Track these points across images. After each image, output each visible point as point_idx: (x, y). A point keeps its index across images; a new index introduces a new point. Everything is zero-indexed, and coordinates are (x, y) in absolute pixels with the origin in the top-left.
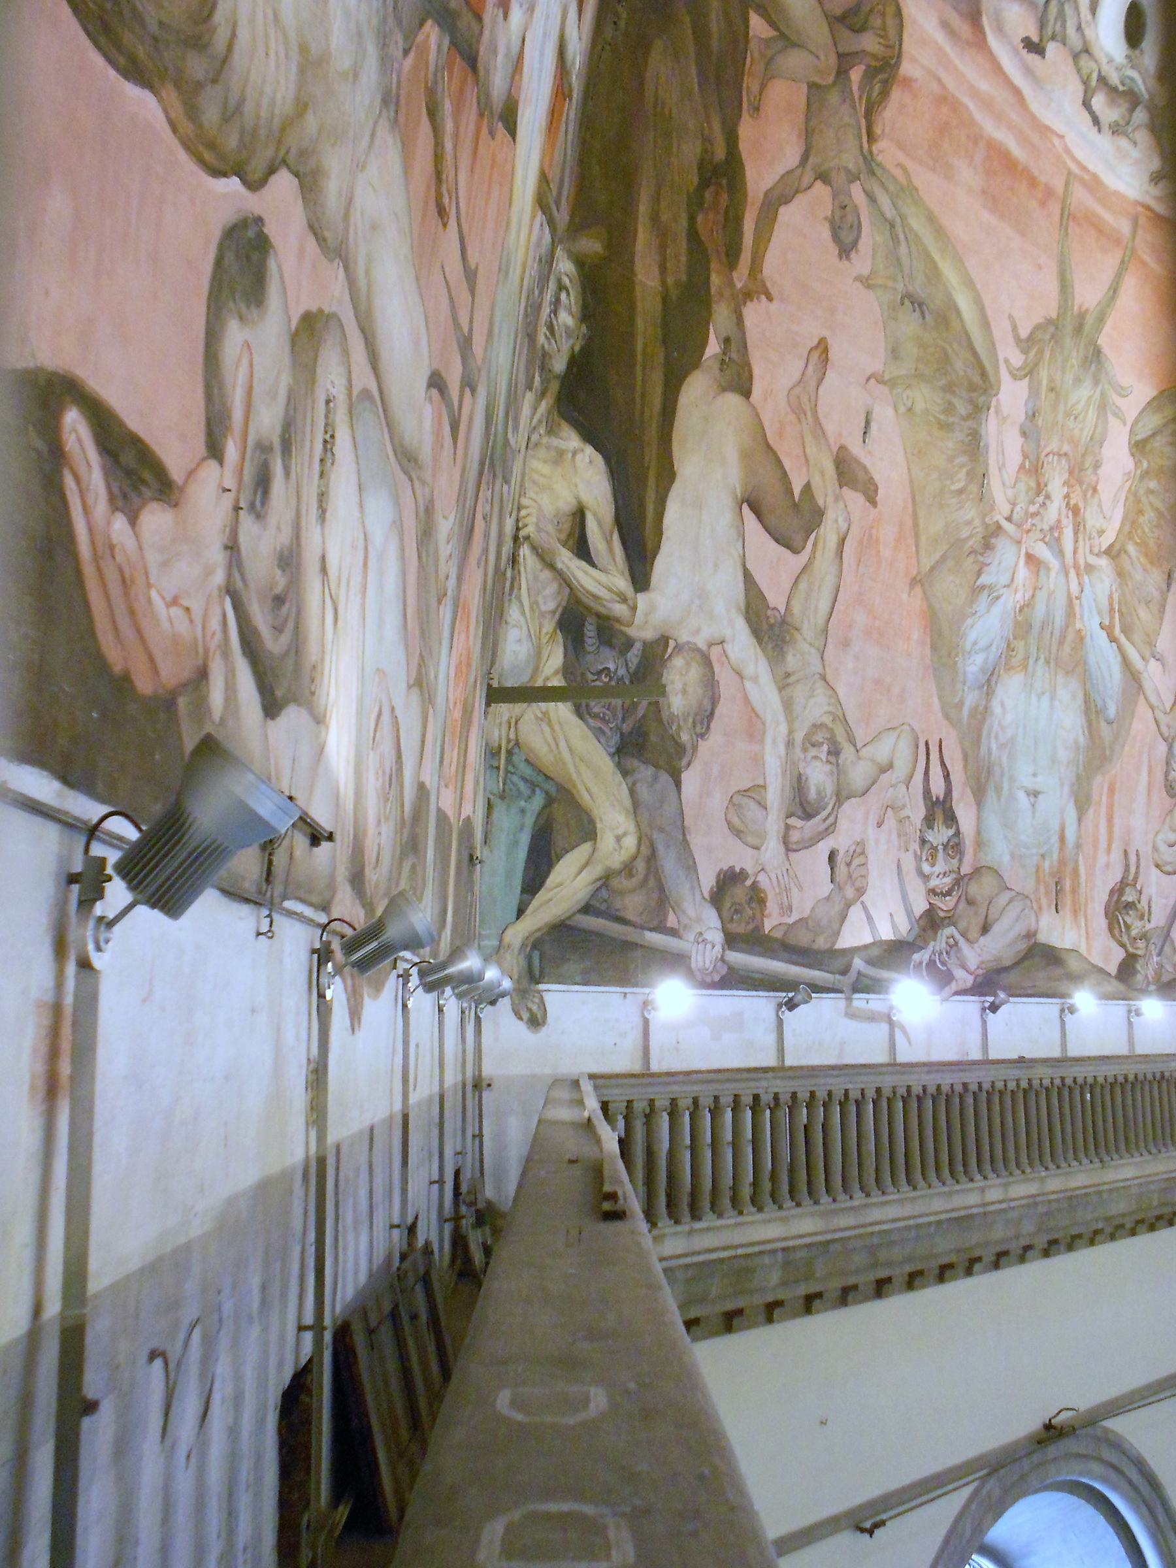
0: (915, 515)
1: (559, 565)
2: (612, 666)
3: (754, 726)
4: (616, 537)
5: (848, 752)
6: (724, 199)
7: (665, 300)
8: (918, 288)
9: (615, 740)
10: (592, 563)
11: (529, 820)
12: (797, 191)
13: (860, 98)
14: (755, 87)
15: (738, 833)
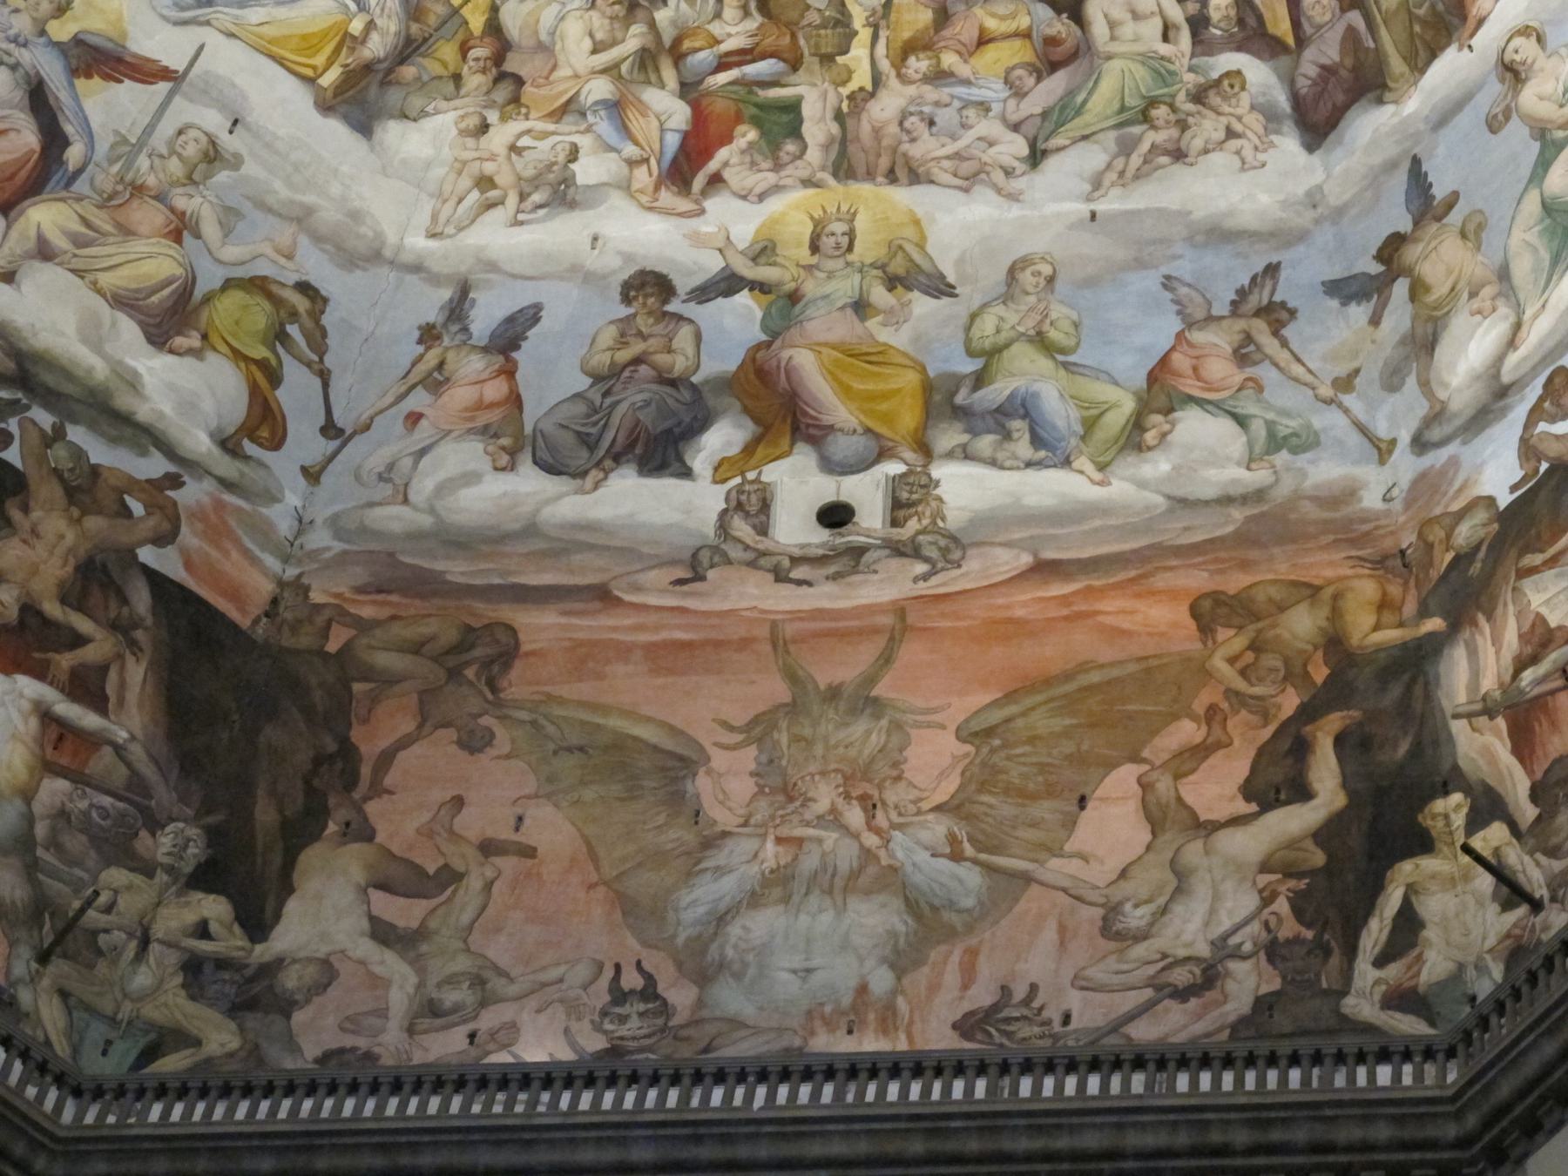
3: (378, 983)
8: (574, 739)
13: (479, 679)
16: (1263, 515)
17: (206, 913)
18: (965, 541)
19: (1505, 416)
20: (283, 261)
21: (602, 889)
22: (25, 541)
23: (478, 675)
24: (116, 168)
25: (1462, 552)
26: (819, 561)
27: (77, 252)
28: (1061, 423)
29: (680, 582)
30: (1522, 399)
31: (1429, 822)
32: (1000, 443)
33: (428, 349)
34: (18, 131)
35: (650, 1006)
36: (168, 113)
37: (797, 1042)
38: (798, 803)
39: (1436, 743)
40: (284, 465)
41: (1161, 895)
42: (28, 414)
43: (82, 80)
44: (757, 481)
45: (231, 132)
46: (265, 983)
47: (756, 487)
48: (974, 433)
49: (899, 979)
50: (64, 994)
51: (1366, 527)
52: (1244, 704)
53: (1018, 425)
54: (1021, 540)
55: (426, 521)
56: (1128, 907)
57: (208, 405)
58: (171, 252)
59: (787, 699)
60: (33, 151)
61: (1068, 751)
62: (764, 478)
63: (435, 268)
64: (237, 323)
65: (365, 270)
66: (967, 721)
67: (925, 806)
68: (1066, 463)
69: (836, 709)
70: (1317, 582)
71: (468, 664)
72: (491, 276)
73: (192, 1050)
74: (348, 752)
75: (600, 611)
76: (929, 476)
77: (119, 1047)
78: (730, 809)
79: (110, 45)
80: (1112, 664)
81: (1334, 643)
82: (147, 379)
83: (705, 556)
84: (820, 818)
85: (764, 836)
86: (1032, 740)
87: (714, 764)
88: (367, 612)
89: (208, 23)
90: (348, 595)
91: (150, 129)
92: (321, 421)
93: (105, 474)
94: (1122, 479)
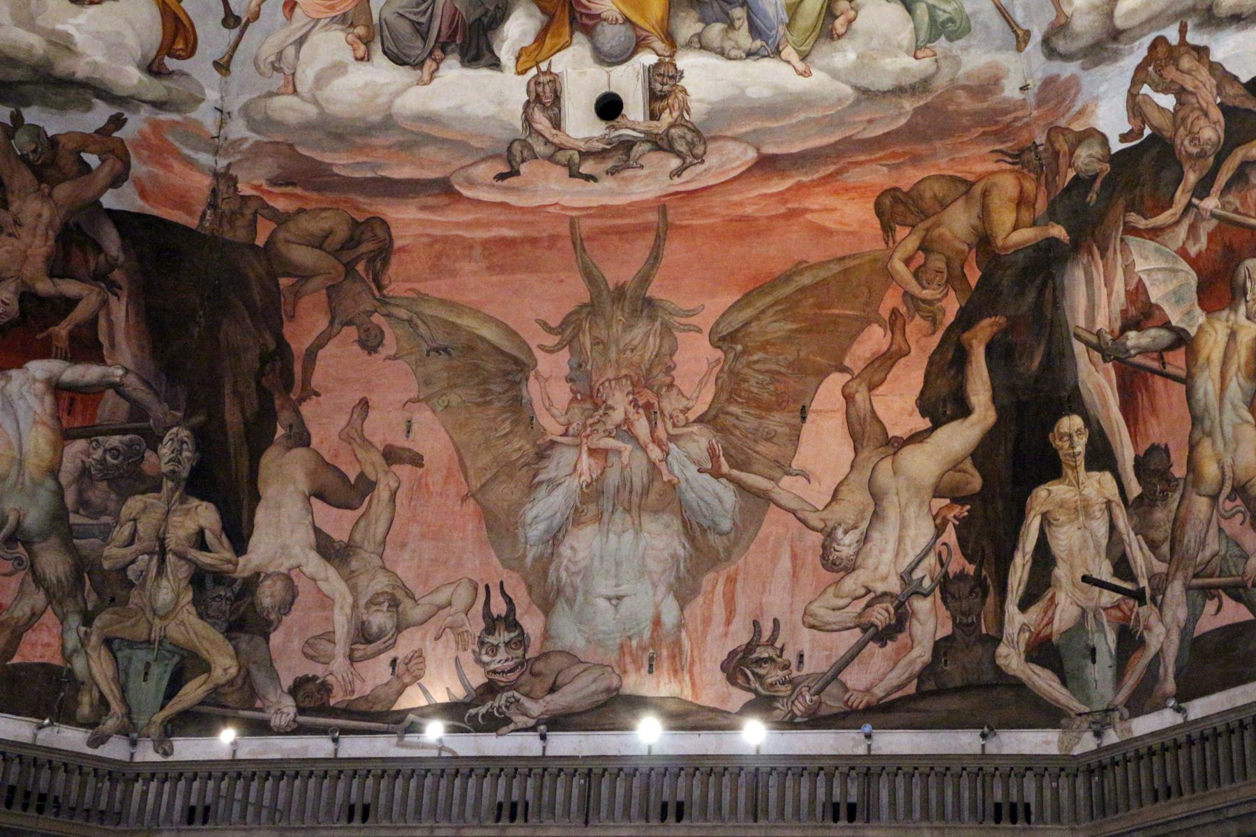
0: (461, 460)
1: (189, 556)
2: (222, 593)
3: (326, 602)
4: (224, 537)
5: (407, 604)
6: (279, 364)
7: (246, 424)
8: (441, 339)
9: (225, 625)
10: (210, 551)
11: (170, 669)
12: (329, 339)
13: (367, 275)
14: (289, 308)
15: (312, 658)
16: (927, 106)
17: (203, 523)
18: (706, 135)
19: (1116, 61)
21: (471, 501)
22: (10, 235)
23: (366, 270)
25: (1082, 175)
26: (600, 155)
28: (771, 11)
29: (501, 177)
30: (1131, 52)
31: (1058, 443)
32: (726, 31)
35: (513, 635)
37: (615, 683)
38: (601, 412)
39: (1062, 354)
40: (199, 67)
41: (863, 519)
44: (548, 72)
46: (249, 600)
47: (548, 78)
48: (706, 21)
49: (682, 609)
50: (108, 642)
51: (1009, 118)
52: (918, 310)
53: (738, 13)
54: (746, 134)
55: (311, 111)
56: (839, 533)
57: (131, 40)
59: (587, 300)
61: (791, 358)
62: (554, 70)
66: (717, 324)
67: (692, 416)
68: (777, 53)
69: (623, 310)
70: (970, 178)
71: (356, 260)
73: (204, 677)
74: (283, 348)
75: (449, 205)
76: (675, 66)
77: (155, 670)
78: (554, 417)
80: (821, 265)
81: (984, 241)
82: (79, 37)
83: (517, 148)
84: (618, 427)
85: (579, 446)
86: (763, 347)
87: (539, 368)
88: (280, 205)
90: (266, 187)
92: (222, 15)
93: (63, 140)
94: (821, 69)
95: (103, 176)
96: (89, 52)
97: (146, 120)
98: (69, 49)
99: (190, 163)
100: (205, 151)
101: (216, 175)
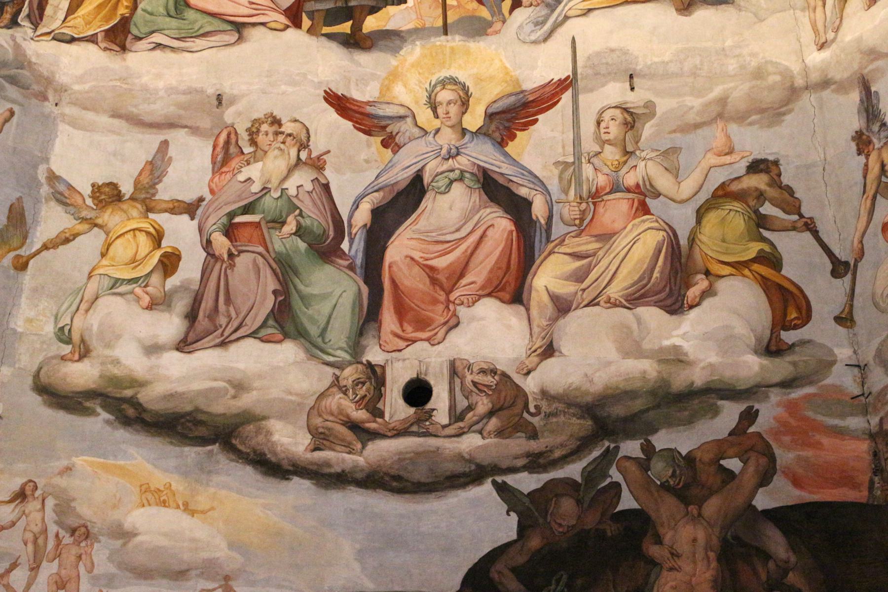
20: (728, 159)
22: (671, 569)
24: (572, 193)
27: (584, 286)
33: (867, 156)
34: (492, 225)
36: (581, 116)
42: (620, 455)
43: (510, 143)
45: (632, 89)
57: (740, 329)
58: (648, 225)
60: (511, 232)
63: (838, 77)
64: (724, 241)
65: (790, 111)
72: (880, 63)
79: (512, 99)
82: (687, 346)
89: (567, 18)
91: (577, 141)
92: (829, 266)
93: (698, 455)
95: (750, 478)
96: (702, 357)
97: (779, 404)
98: (681, 361)
99: (839, 433)
100: (852, 415)
101: (872, 436)
